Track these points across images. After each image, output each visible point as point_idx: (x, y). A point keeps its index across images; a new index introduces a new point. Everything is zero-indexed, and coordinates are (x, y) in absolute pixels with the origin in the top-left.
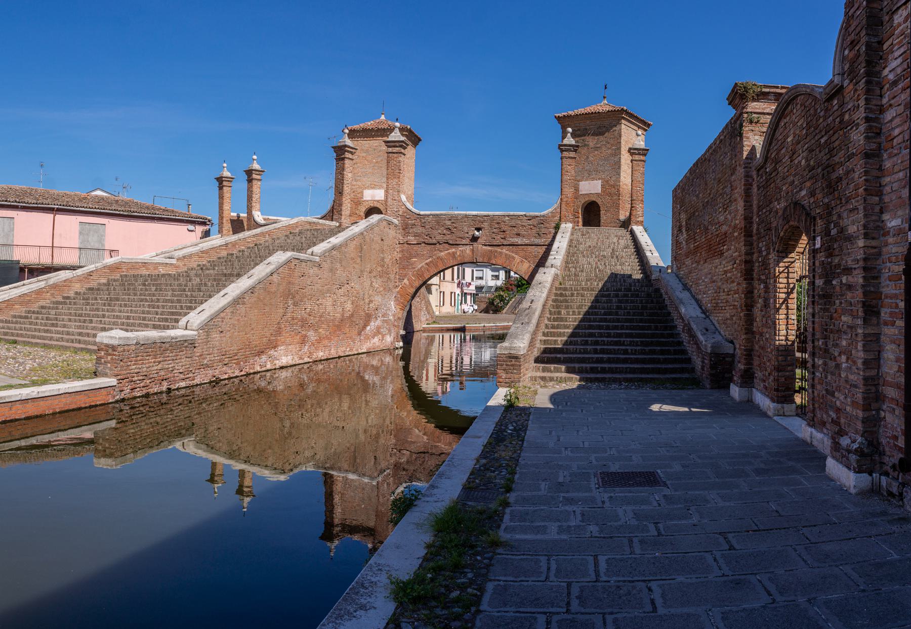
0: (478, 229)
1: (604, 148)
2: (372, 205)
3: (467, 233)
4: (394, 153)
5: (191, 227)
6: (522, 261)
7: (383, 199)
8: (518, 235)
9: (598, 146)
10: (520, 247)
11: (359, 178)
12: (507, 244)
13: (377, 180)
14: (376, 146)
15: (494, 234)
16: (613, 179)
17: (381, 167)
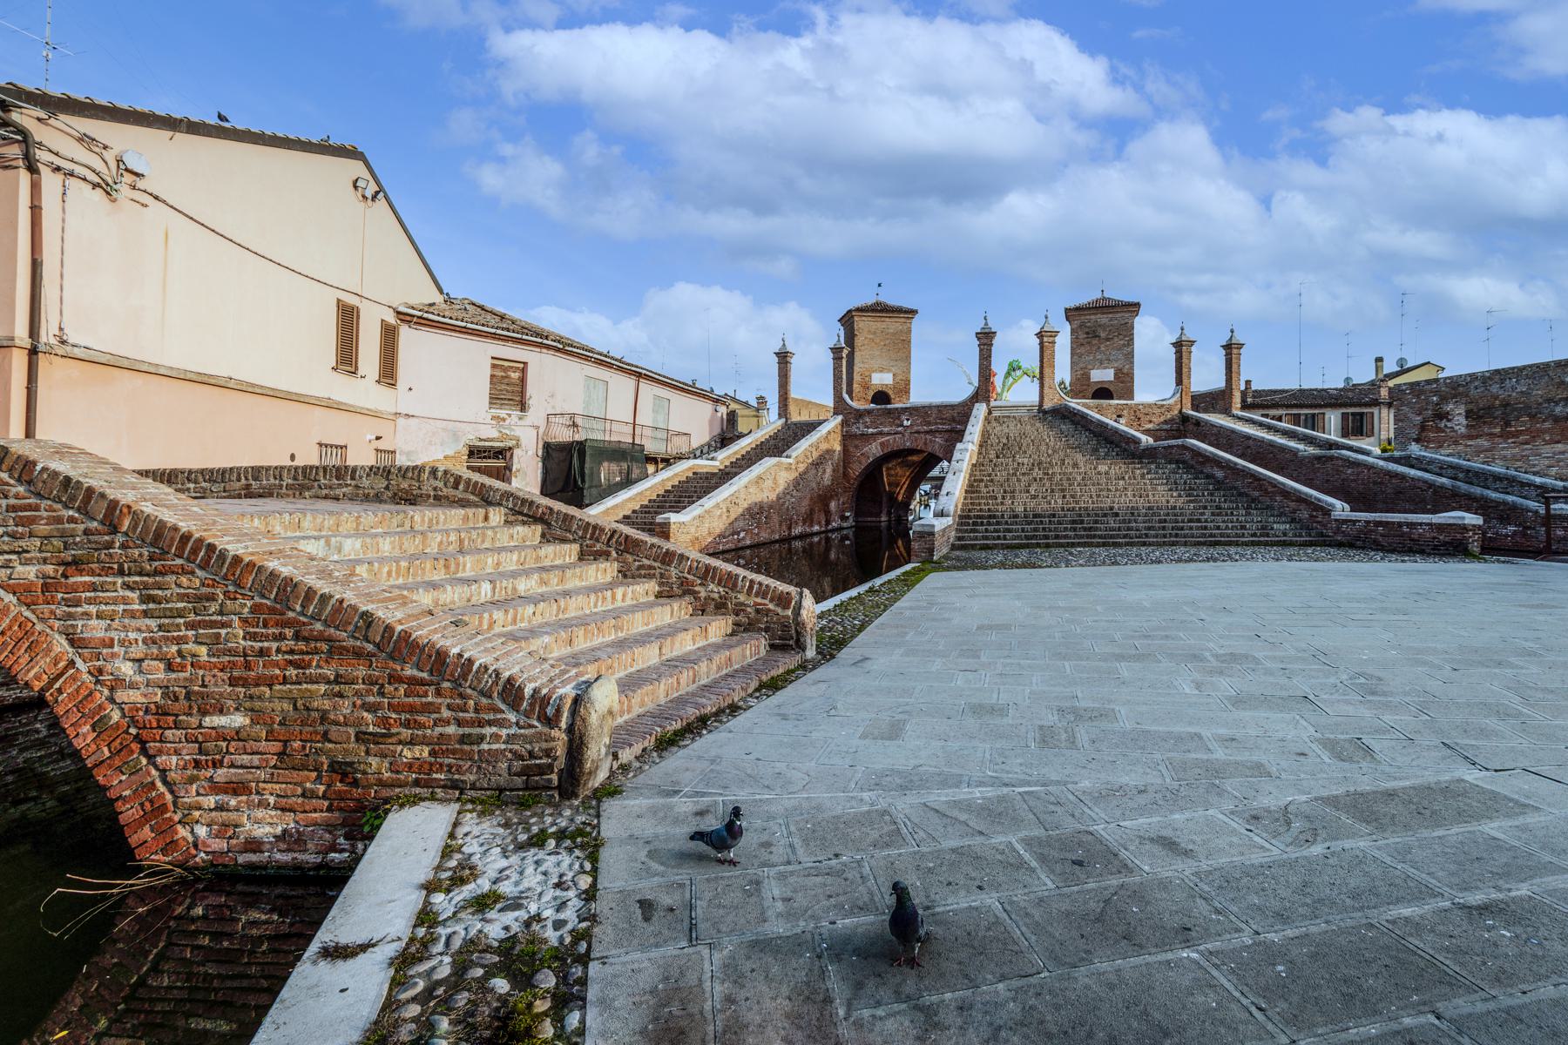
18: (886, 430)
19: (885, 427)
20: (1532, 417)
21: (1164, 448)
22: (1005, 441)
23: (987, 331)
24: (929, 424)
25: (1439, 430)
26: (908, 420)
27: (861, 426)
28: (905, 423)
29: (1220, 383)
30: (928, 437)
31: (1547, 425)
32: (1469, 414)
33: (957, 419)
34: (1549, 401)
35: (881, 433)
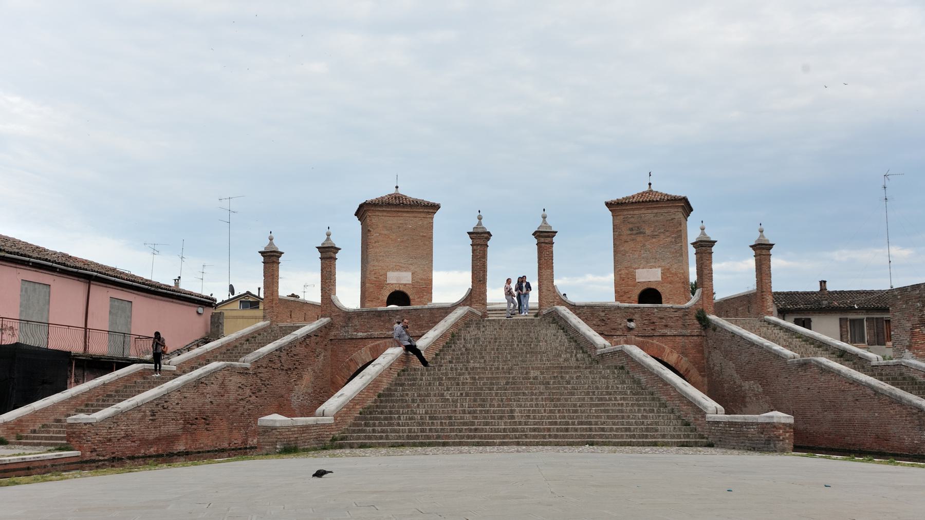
0: (630, 320)
1: (662, 236)
2: (398, 289)
3: (620, 324)
4: (546, 243)
5: (200, 310)
6: (671, 352)
7: (411, 283)
8: (666, 326)
9: (656, 233)
10: (668, 338)
11: (381, 258)
12: (659, 334)
13: (402, 261)
14: (400, 224)
15: (645, 326)
16: (675, 266)
17: (407, 247)
18: (376, 334)
23: (480, 230)
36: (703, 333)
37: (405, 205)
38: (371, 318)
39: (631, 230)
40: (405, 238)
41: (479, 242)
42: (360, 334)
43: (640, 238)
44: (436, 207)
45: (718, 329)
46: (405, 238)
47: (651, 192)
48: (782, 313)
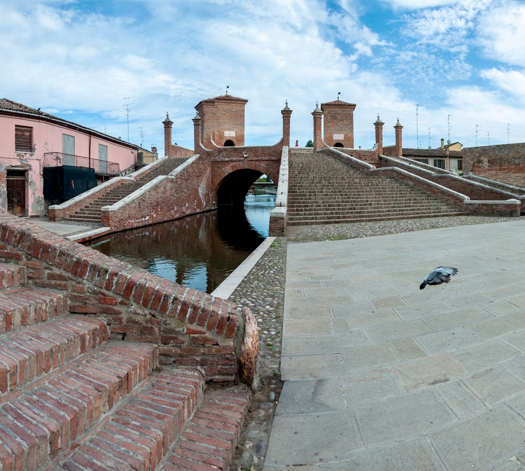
1: (345, 121)
16: (350, 134)
18: (234, 159)
19: (234, 157)
20: (509, 163)
21: (383, 171)
22: (301, 165)
23: (287, 110)
24: (257, 156)
25: (479, 167)
26: (246, 154)
27: (221, 157)
28: (245, 155)
29: (393, 143)
30: (257, 163)
31: (513, 167)
32: (489, 161)
33: (272, 154)
34: (514, 158)
35: (232, 161)
36: (379, 163)
37: (232, 100)
38: (231, 151)
39: (332, 117)
40: (233, 115)
41: (286, 115)
42: (226, 159)
43: (335, 121)
44: (246, 101)
45: (389, 161)
46: (233, 115)
47: (338, 101)
48: (403, 155)
